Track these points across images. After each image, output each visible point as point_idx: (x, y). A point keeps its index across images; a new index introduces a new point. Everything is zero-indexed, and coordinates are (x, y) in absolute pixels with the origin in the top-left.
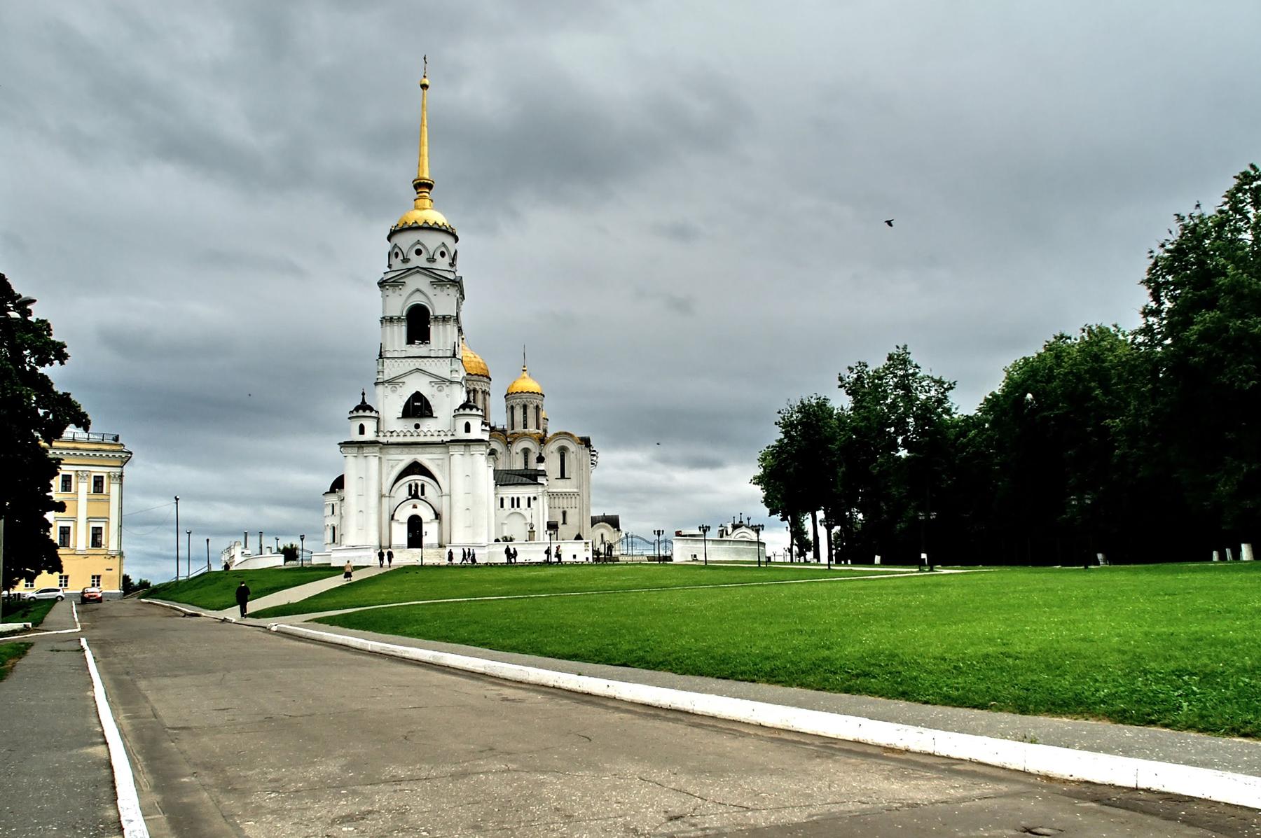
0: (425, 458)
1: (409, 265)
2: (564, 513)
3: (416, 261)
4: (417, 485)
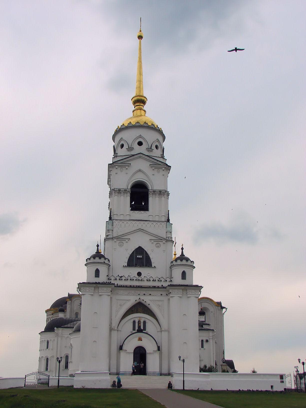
0: (150, 300)
1: (133, 153)
3: (137, 149)
4: (139, 322)
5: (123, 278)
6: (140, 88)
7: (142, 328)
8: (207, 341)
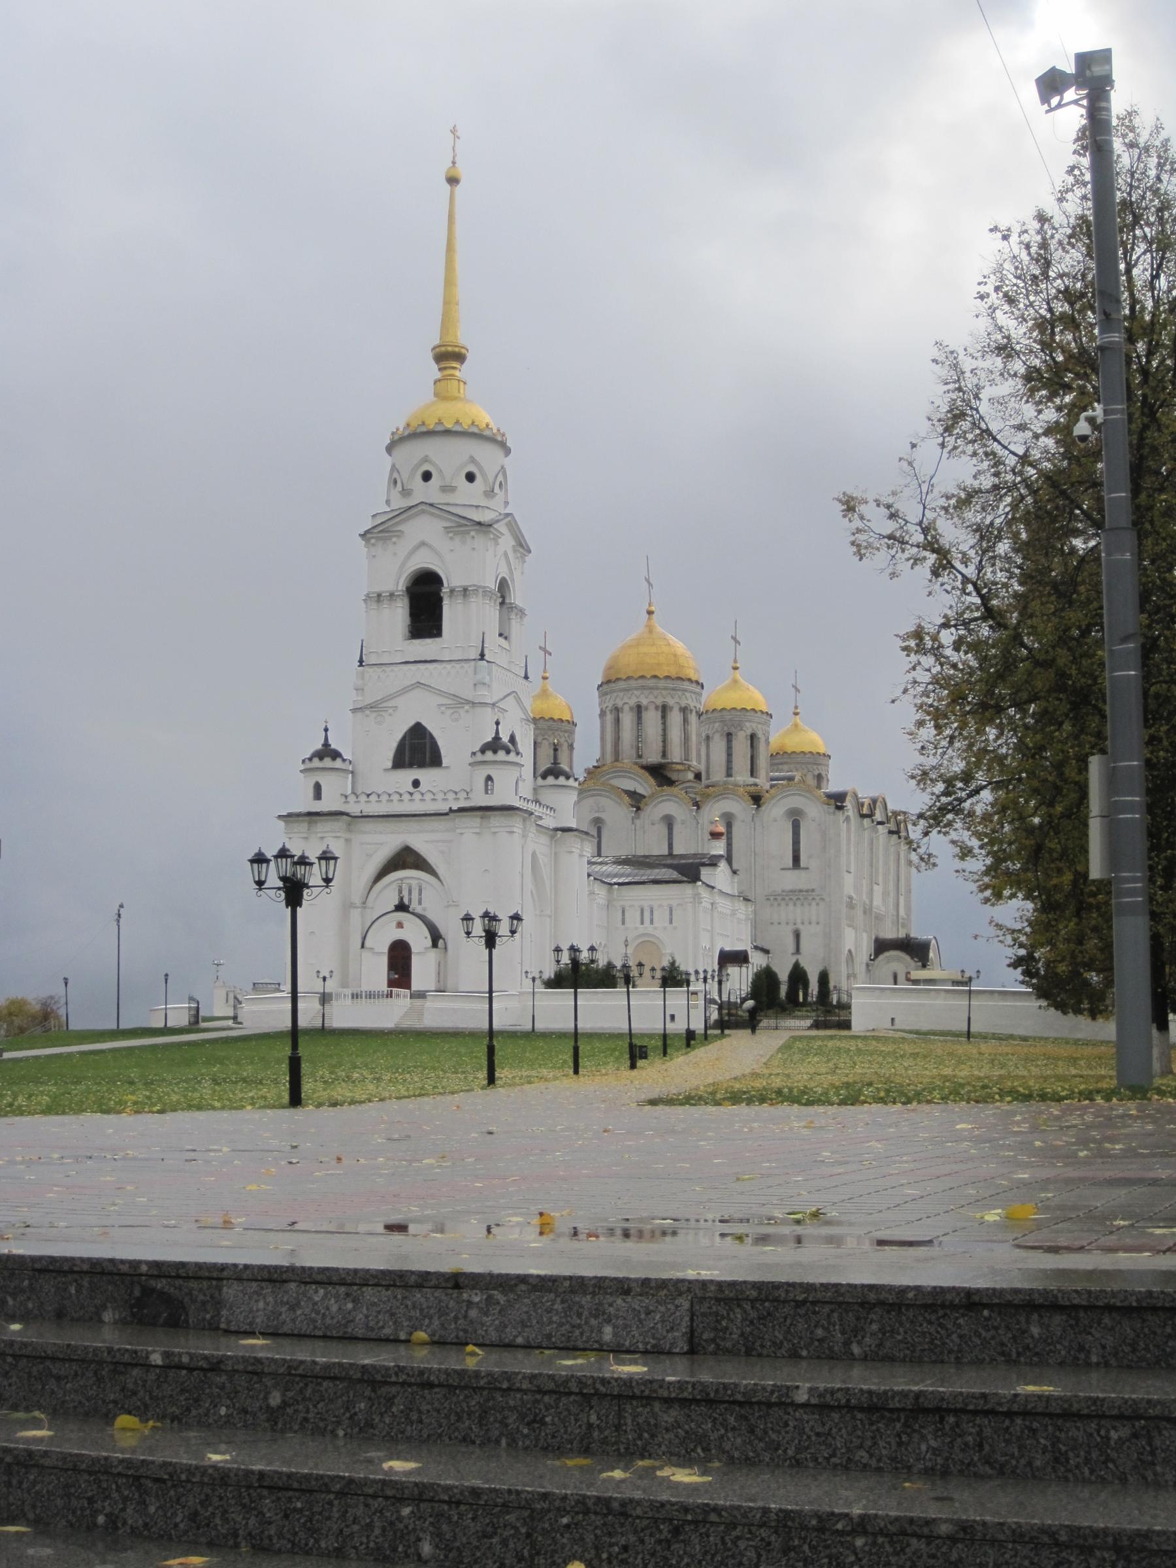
2: (797, 935)
3: (422, 492)
5: (373, 798)
6: (447, 321)
7: (406, 901)
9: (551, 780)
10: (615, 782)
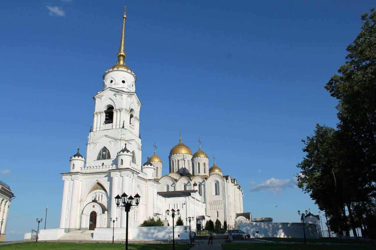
5: (89, 168)
7: (97, 199)
8: (185, 204)
9: (146, 166)
10: (172, 177)
